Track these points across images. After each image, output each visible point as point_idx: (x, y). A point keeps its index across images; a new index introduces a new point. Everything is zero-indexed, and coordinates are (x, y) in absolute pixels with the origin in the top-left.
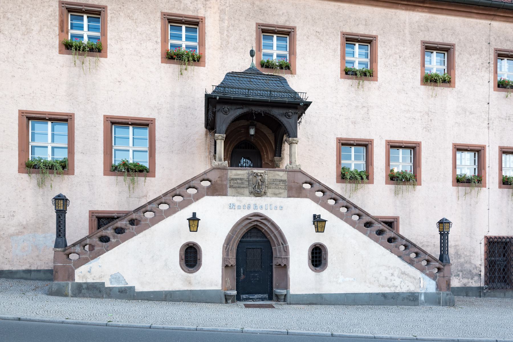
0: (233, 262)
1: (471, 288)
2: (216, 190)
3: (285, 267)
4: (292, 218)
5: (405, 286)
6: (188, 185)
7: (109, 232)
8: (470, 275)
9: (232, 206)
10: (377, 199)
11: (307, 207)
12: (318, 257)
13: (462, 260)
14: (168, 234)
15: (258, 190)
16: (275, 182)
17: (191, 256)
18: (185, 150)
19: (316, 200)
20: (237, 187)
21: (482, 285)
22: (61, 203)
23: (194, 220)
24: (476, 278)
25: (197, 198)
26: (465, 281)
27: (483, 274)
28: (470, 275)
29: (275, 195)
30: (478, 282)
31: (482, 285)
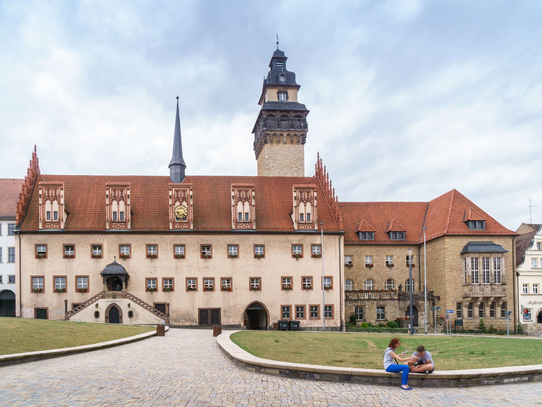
0: (108, 316)
2: (103, 297)
3: (122, 317)
4: (123, 304)
6: (96, 296)
7: (77, 308)
9: (107, 301)
10: (160, 297)
11: (127, 301)
12: (131, 314)
14: (91, 309)
15: (114, 297)
16: (119, 295)
17: (97, 314)
18: (97, 285)
19: (130, 299)
20: (108, 296)
22: (66, 301)
23: (97, 305)
25: (98, 299)
27: (197, 321)
28: (192, 321)
31: (197, 324)
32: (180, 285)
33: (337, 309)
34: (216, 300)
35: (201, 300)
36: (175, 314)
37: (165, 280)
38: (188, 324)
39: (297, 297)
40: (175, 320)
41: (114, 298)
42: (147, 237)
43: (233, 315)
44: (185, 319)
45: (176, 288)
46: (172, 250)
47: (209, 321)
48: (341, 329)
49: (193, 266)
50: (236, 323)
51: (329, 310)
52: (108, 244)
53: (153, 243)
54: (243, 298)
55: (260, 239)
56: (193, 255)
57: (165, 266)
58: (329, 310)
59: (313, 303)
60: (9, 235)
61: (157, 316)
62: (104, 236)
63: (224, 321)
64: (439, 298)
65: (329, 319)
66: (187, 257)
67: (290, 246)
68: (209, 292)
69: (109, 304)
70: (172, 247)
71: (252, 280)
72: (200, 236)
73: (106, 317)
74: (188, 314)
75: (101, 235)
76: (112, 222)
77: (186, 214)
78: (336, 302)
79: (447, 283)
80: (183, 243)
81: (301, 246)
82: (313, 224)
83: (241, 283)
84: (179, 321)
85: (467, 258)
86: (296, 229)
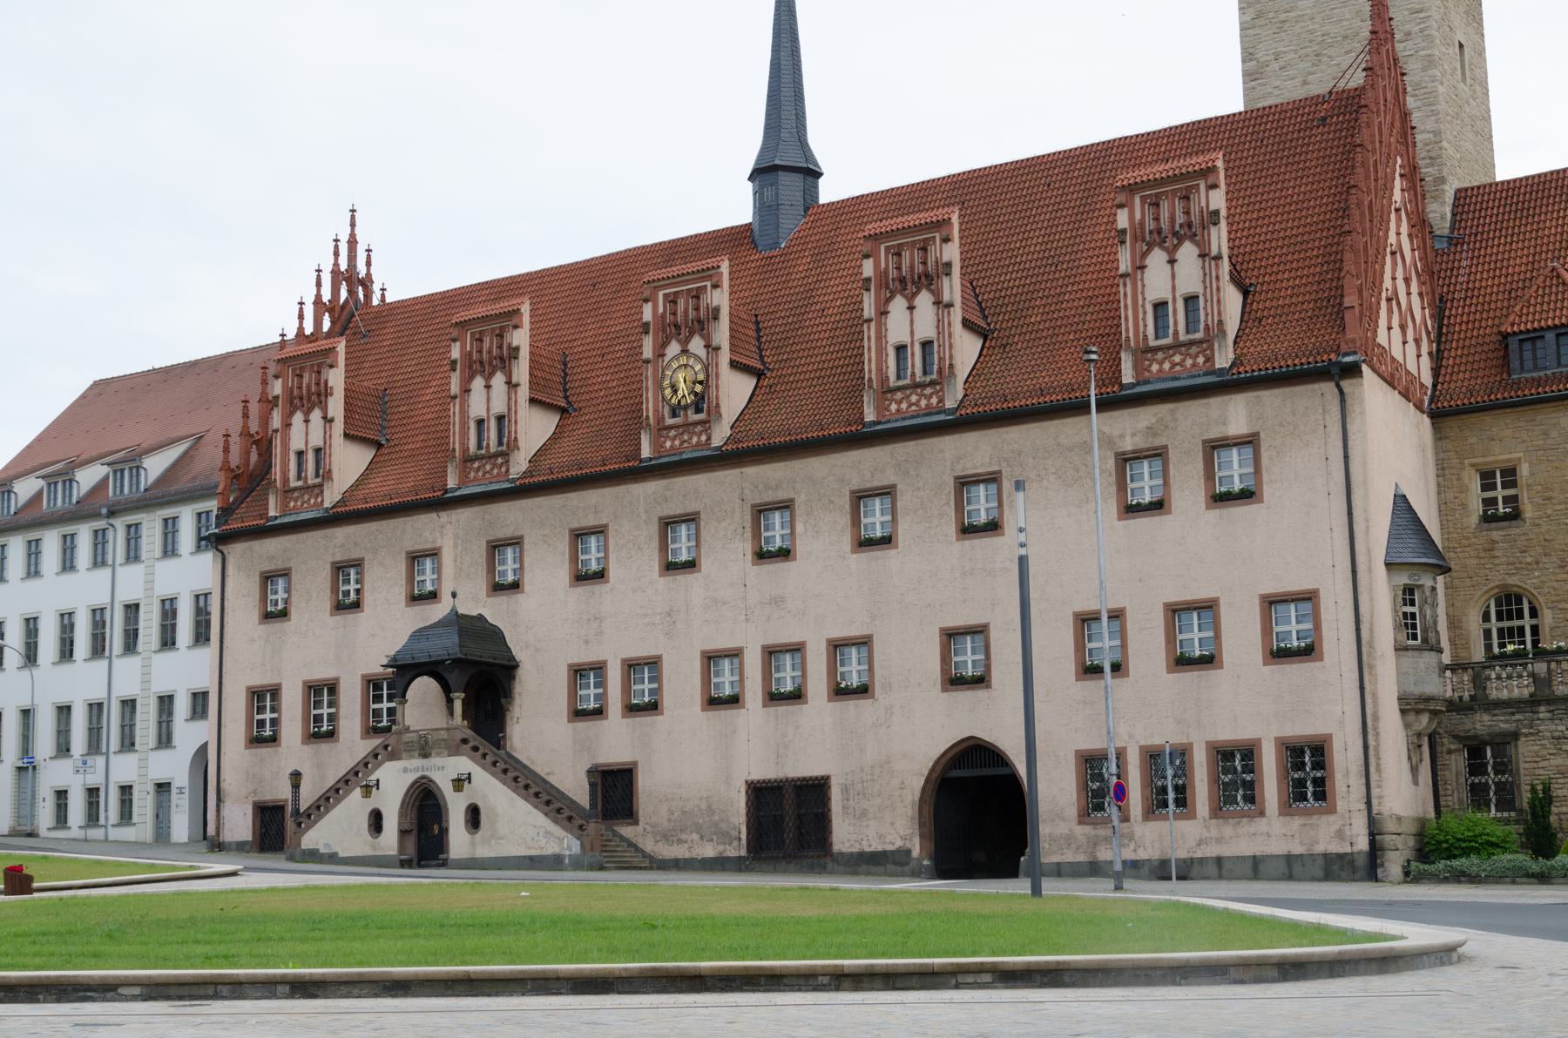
1: (728, 859)
2: (394, 756)
5: (551, 848)
8: (725, 837)
9: (405, 770)
10: (615, 741)
12: (474, 816)
13: (716, 818)
21: (743, 852)
24: (735, 843)
26: (721, 848)
27: (744, 836)
28: (725, 837)
29: (438, 755)
30: (738, 850)
31: (743, 852)
32: (682, 684)
34: (809, 743)
35: (763, 746)
36: (664, 810)
37: (632, 667)
38: (709, 851)
39: (1151, 710)
40: (666, 837)
41: (425, 756)
42: (574, 499)
43: (881, 808)
44: (698, 829)
45: (667, 701)
46: (655, 543)
47: (789, 836)
48: (1370, 866)
49: (729, 602)
50: (893, 842)
51: (1308, 768)
52: (456, 546)
53: (591, 521)
54: (917, 728)
55: (976, 450)
56: (726, 553)
57: (637, 609)
58: (1308, 768)
59: (1230, 732)
60: (199, 548)
61: (556, 821)
62: (445, 517)
63: (845, 835)
65: (1309, 813)
66: (705, 564)
68: (783, 709)
69: (411, 777)
70: (654, 528)
71: (951, 636)
72: (751, 471)
73: (403, 833)
74: (710, 810)
75: (434, 515)
76: (468, 459)
77: (698, 388)
78: (1341, 723)
80: (691, 507)
81: (1158, 454)
83: (907, 657)
84: (680, 841)
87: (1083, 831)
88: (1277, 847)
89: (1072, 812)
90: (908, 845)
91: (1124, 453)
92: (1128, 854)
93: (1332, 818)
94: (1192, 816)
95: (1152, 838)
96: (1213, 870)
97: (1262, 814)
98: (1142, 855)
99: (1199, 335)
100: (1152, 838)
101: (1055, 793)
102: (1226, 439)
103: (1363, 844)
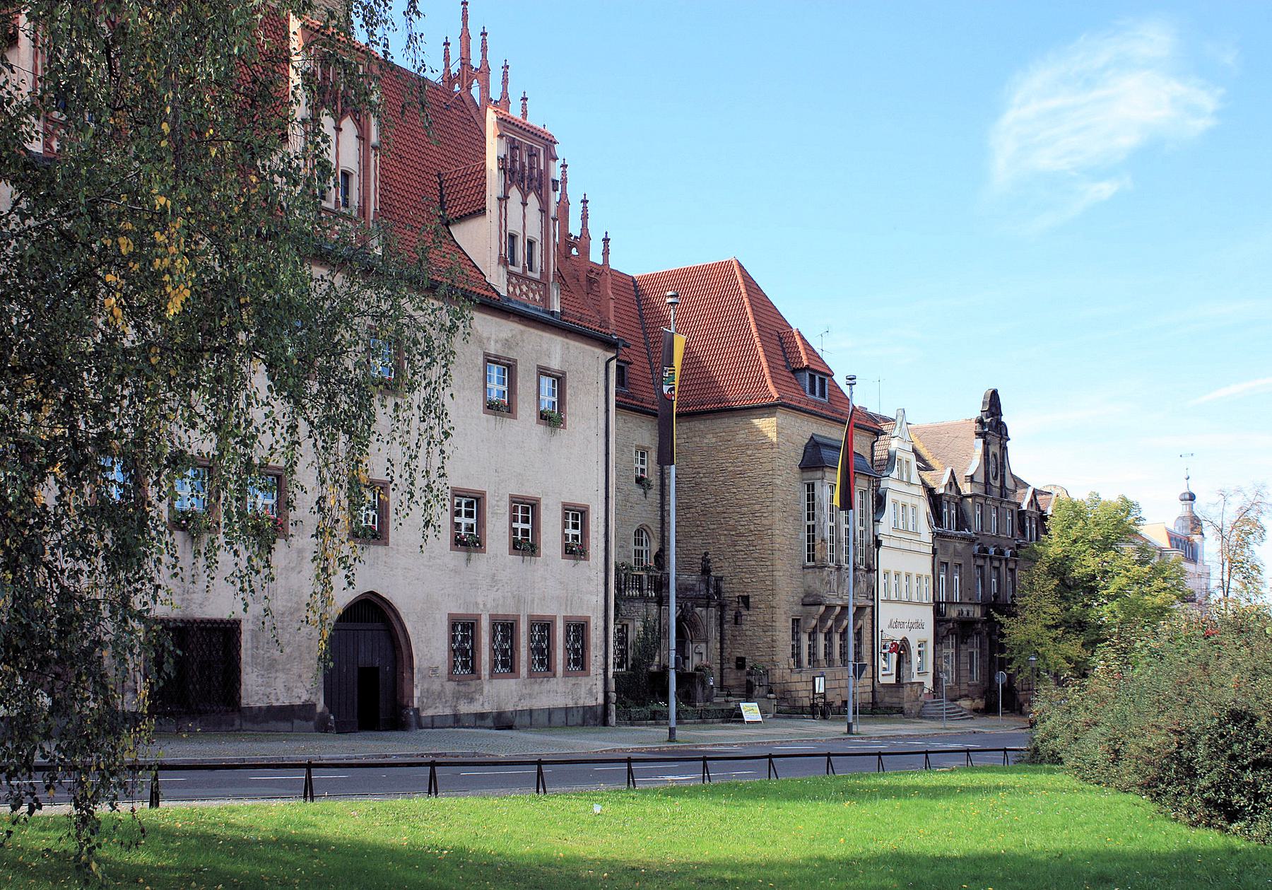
33: (595, 636)
63: (256, 688)
64: (745, 600)
67: (480, 360)
79: (777, 554)
82: (543, 283)
85: (818, 484)
86: (504, 293)
87: (450, 686)
88: (560, 701)
89: (444, 669)
90: (313, 699)
91: (489, 355)
92: (476, 708)
93: (586, 679)
94: (518, 677)
95: (501, 693)
96: (526, 720)
97: (554, 676)
98: (487, 709)
99: (537, 276)
100: (501, 693)
101: (429, 647)
102: (548, 369)
103: (601, 700)
